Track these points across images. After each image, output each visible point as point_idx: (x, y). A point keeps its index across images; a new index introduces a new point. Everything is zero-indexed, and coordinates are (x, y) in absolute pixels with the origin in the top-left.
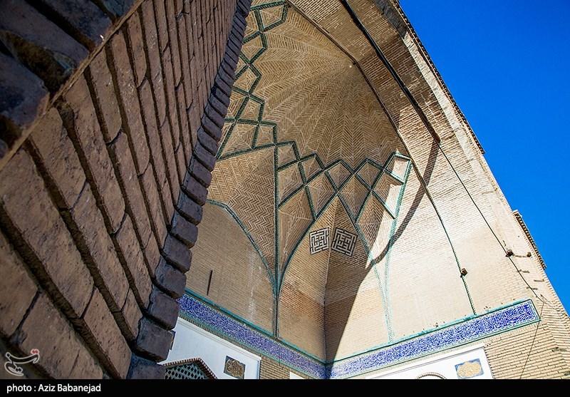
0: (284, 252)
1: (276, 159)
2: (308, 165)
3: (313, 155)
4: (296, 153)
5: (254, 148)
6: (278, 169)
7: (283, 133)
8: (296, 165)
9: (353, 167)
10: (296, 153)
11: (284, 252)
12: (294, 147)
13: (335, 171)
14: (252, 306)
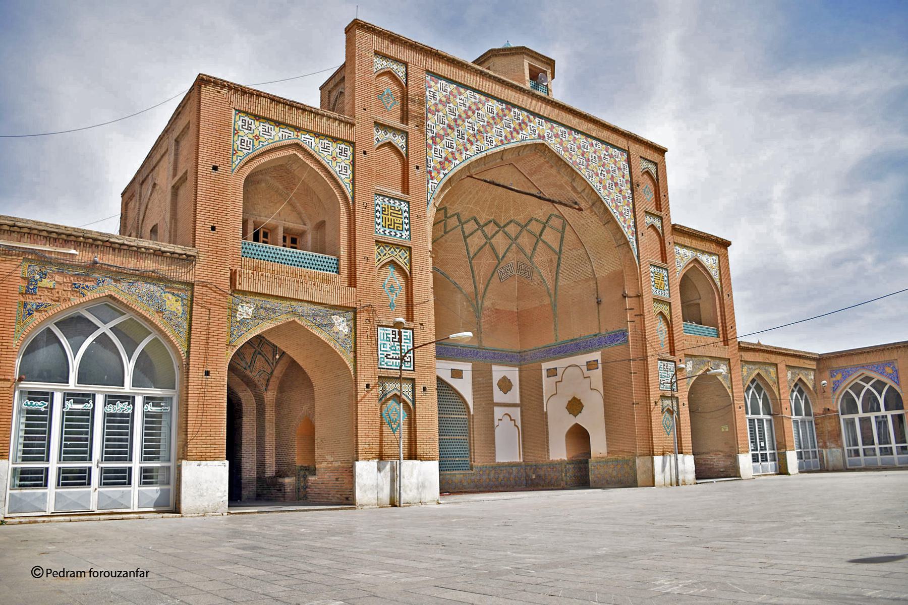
0: (481, 287)
1: (463, 232)
2: (490, 229)
3: (490, 222)
4: (478, 223)
5: (446, 233)
6: (465, 238)
8: (480, 231)
9: (523, 224)
10: (478, 223)
11: (481, 287)
12: (476, 220)
13: (512, 229)
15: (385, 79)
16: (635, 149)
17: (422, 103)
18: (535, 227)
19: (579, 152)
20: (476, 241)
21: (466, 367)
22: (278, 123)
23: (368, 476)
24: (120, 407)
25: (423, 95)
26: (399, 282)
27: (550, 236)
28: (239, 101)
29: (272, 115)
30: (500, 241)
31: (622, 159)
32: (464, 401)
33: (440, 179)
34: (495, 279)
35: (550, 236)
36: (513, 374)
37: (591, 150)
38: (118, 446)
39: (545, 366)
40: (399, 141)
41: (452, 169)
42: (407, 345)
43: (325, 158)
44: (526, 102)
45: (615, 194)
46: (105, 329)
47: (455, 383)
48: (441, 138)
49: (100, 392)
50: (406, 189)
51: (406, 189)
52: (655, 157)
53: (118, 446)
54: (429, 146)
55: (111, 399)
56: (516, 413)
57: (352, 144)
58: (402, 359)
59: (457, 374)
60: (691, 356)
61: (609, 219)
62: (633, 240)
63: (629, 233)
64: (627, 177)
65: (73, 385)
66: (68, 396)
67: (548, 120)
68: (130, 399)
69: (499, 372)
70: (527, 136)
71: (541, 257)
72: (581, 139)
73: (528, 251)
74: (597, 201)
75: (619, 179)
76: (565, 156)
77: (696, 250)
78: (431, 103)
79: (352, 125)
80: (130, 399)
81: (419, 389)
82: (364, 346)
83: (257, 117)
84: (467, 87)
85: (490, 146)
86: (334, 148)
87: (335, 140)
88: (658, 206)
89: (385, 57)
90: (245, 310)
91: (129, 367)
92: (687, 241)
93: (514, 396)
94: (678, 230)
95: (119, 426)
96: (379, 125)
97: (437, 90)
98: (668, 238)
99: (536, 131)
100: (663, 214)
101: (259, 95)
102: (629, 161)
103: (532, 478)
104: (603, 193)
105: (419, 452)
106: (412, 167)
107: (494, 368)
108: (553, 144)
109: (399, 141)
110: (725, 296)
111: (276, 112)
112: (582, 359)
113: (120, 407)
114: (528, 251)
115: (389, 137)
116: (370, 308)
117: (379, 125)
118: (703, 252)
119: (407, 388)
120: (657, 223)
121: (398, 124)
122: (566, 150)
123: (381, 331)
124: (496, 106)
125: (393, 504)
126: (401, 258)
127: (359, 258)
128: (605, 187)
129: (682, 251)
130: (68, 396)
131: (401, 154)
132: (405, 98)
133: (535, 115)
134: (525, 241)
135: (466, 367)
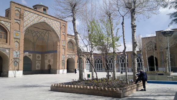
2: (36, 33)
5: (29, 33)
7: (32, 30)
14: (31, 49)
15: (17, 11)
16: (61, 21)
17: (23, 16)
18: (44, 33)
19: (51, 22)
20: (34, 34)
21: (31, 55)
23: (11, 73)
25: (23, 14)
26: (18, 44)
30: (38, 34)
31: (59, 23)
32: (31, 60)
33: (25, 29)
34: (38, 40)
35: (46, 34)
36: (40, 55)
37: (53, 22)
39: (45, 55)
40: (19, 22)
41: (28, 26)
42: (18, 54)
44: (42, 14)
45: (57, 29)
47: (30, 57)
50: (20, 30)
51: (20, 30)
52: (66, 23)
54: (24, 23)
56: (40, 62)
57: (10, 23)
58: (17, 56)
59: (30, 55)
61: (56, 33)
62: (59, 37)
63: (59, 36)
64: (60, 26)
67: (46, 17)
69: (37, 55)
70: (42, 20)
71: (45, 37)
72: (52, 20)
73: (43, 36)
74: (54, 31)
76: (48, 23)
77: (71, 38)
78: (25, 15)
79: (11, 20)
81: (20, 60)
82: (11, 54)
84: (31, 12)
85: (36, 21)
88: (65, 31)
92: (69, 36)
93: (40, 59)
94: (68, 35)
96: (15, 19)
97: (26, 13)
98: (66, 36)
99: (43, 19)
100: (66, 32)
102: (60, 24)
103: (42, 71)
104: (55, 29)
105: (19, 69)
106: (21, 26)
108: (46, 22)
109: (19, 22)
112: (51, 54)
114: (43, 36)
115: (17, 21)
116: (12, 48)
117: (15, 19)
119: (18, 60)
120: (64, 34)
121: (19, 19)
122: (49, 22)
123: (14, 52)
125: (15, 77)
126: (18, 41)
127: (11, 41)
131: (19, 24)
132: (20, 15)
133: (44, 17)
135: (31, 55)
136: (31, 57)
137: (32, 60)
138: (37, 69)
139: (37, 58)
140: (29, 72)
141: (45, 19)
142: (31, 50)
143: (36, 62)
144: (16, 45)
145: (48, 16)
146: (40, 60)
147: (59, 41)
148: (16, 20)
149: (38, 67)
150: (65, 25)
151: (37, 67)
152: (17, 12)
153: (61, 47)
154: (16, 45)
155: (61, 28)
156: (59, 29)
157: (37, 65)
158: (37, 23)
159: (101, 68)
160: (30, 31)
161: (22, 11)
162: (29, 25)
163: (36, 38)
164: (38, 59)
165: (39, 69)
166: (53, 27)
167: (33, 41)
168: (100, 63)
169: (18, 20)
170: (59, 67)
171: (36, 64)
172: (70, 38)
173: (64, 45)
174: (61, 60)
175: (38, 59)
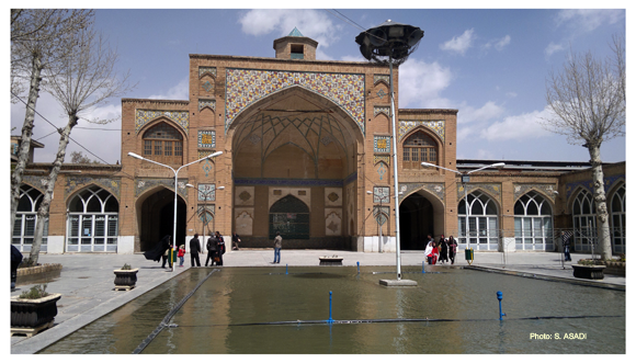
2: (308, 122)
14: (306, 173)
21: (308, 190)
22: (154, 110)
24: (100, 219)
25: (224, 79)
27: (333, 124)
28: (138, 105)
29: (151, 108)
30: (314, 126)
31: (358, 80)
35: (333, 124)
36: (339, 192)
38: (100, 230)
40: (211, 105)
43: (176, 120)
44: (288, 67)
46: (95, 194)
47: (302, 198)
48: (234, 98)
49: (94, 214)
53: (100, 230)
55: (97, 216)
56: (340, 211)
59: (303, 193)
60: (405, 183)
61: (346, 116)
65: (85, 212)
66: (84, 216)
67: (301, 72)
68: (104, 216)
69: (328, 191)
70: (287, 84)
72: (326, 77)
74: (336, 108)
75: (354, 91)
76: (313, 89)
78: (229, 84)
80: (104, 216)
83: (145, 110)
84: (249, 69)
86: (180, 115)
87: (180, 111)
89: (205, 67)
90: (142, 184)
91: (103, 206)
92: (412, 117)
93: (339, 202)
94: (402, 112)
95: (100, 225)
97: (233, 75)
101: (145, 101)
102: (364, 80)
107: (326, 189)
108: (305, 85)
110: (447, 145)
111: (153, 106)
113: (100, 219)
115: (207, 103)
118: (429, 121)
121: (212, 97)
124: (267, 74)
128: (342, 99)
129: (406, 123)
130: (84, 216)
132: (217, 84)
133: (293, 72)
134: (325, 126)
135: (308, 190)
136: (306, 199)
137: (309, 205)
138: (329, 232)
139: (327, 199)
140: (300, 242)
141: (300, 77)
142: (306, 175)
143: (324, 212)
144: (207, 169)
145: (308, 66)
146: (339, 207)
147: (362, 141)
148: (205, 100)
149: (333, 226)
150: (386, 79)
151: (329, 227)
152: (206, 80)
153: (369, 157)
154: (207, 169)
155: (367, 93)
156: (360, 97)
157: (328, 222)
158: (272, 97)
159: (106, 237)
160: (286, 122)
161: (219, 74)
162: (244, 107)
163: (313, 138)
164: (331, 203)
165: (338, 232)
166: (334, 99)
167: (309, 150)
168: (484, 215)
169: (210, 101)
170: (363, 228)
171: (324, 219)
172: (414, 124)
173: (380, 151)
174: (369, 204)
175: (331, 203)
